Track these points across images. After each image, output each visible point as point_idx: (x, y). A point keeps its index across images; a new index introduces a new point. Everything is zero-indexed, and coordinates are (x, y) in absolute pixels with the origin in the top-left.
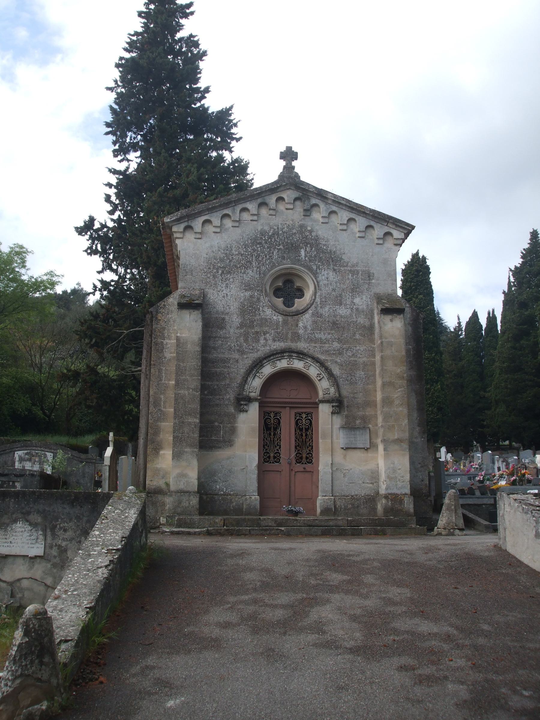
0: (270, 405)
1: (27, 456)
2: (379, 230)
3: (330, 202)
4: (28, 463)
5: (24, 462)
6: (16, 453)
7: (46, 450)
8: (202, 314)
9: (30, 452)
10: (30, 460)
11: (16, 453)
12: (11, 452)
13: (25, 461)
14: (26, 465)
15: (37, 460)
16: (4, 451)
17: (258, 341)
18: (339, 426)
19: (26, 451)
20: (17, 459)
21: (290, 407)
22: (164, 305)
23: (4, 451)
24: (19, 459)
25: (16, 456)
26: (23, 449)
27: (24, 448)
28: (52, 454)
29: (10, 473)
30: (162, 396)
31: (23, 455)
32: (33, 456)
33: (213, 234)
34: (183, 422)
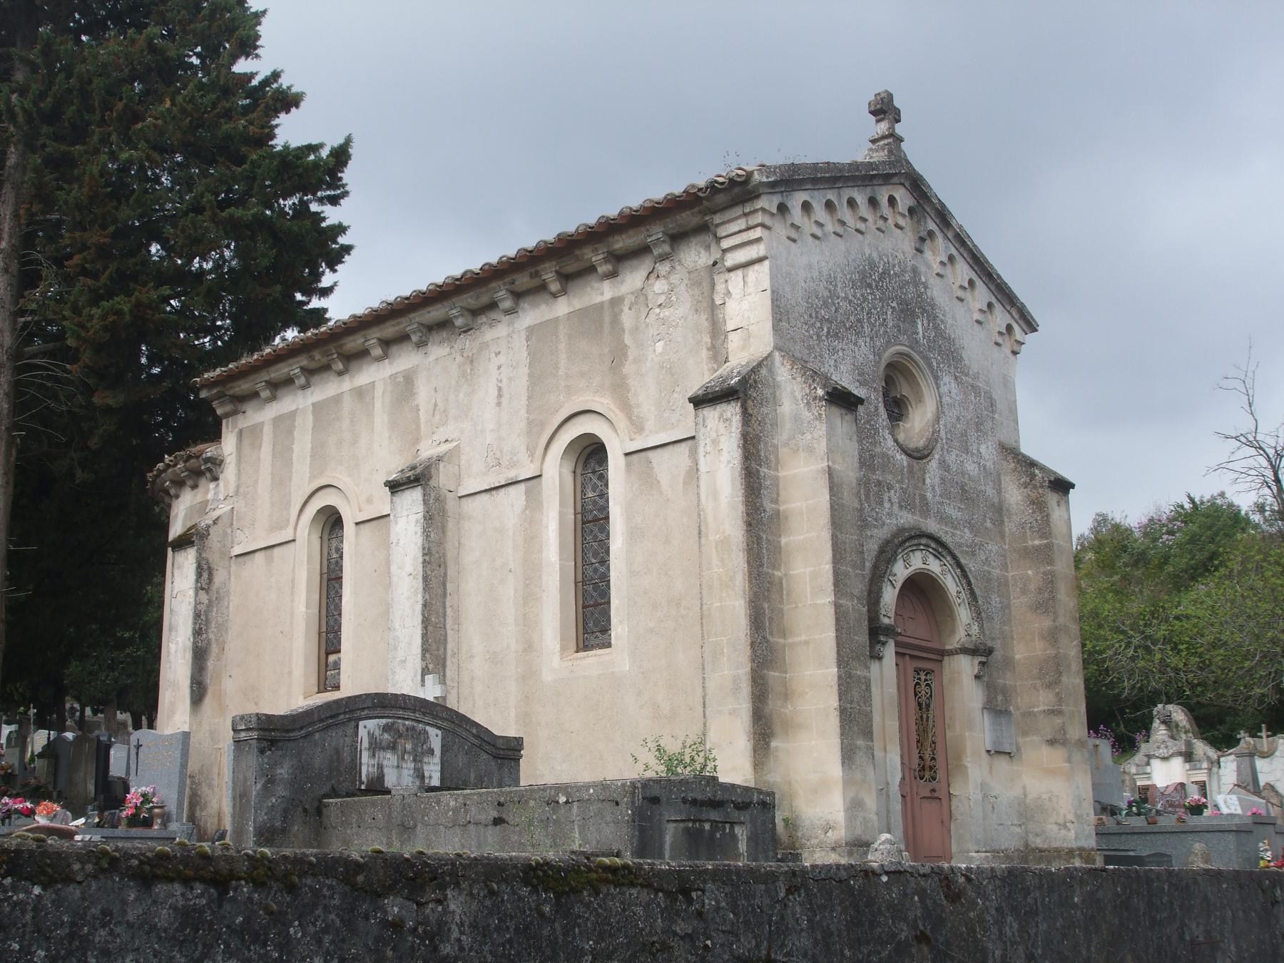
0: (924, 655)
1: (386, 736)
2: (1001, 318)
3: (950, 235)
4: (389, 755)
5: (382, 754)
6: (361, 724)
7: (426, 719)
8: (746, 416)
9: (393, 724)
10: (392, 747)
11: (361, 724)
12: (350, 720)
13: (384, 749)
14: (385, 763)
15: (409, 747)
16: (331, 717)
17: (881, 503)
18: (980, 706)
19: (384, 721)
20: (366, 744)
21: (912, 657)
22: (755, 381)
23: (331, 717)
24: (370, 744)
25: (362, 733)
26: (376, 712)
27: (378, 712)
28: (439, 732)
29: (726, 797)
30: (766, 605)
31: (377, 733)
32: (400, 736)
33: (811, 239)
34: (850, 677)
